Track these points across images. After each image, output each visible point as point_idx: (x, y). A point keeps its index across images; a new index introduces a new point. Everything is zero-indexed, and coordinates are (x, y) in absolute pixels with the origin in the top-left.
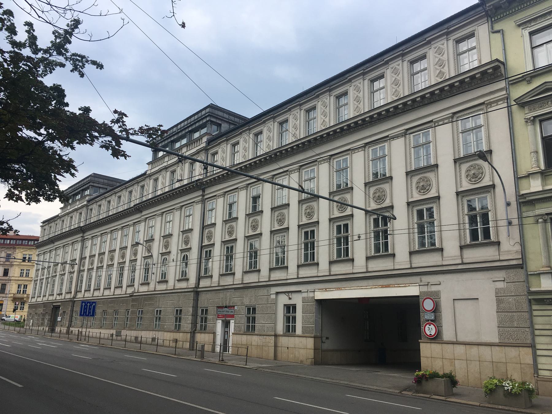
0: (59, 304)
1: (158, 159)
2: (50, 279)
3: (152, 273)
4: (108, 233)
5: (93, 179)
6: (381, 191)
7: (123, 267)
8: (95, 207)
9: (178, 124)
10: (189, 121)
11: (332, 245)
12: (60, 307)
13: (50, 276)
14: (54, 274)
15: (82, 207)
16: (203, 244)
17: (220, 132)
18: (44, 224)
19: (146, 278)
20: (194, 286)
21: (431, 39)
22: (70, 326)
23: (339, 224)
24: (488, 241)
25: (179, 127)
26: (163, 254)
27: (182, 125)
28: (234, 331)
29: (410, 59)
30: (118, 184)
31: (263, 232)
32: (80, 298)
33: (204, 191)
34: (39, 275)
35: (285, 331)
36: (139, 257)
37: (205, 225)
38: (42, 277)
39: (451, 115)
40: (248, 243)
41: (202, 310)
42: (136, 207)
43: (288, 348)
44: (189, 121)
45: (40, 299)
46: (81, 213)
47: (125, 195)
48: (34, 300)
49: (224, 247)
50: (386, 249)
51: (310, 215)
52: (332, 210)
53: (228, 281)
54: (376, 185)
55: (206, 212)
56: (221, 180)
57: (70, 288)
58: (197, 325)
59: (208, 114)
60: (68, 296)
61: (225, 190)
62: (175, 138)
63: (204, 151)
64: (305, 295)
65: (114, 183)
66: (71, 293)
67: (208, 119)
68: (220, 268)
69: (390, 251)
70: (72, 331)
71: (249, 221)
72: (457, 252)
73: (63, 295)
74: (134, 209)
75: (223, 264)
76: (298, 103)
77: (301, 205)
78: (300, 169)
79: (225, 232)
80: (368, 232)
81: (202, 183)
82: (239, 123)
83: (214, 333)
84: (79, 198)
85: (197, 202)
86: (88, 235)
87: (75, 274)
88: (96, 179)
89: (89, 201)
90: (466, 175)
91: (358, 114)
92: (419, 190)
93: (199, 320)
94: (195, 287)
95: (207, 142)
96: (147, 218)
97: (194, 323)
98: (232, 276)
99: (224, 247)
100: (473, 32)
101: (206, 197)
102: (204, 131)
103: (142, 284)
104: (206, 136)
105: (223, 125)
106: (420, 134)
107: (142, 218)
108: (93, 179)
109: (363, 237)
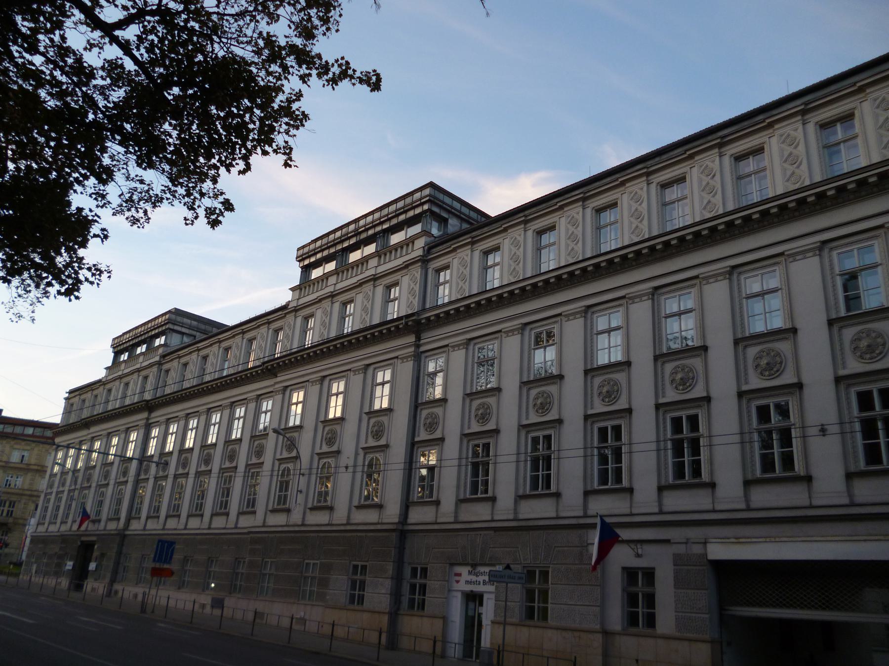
0: (94, 538)
1: (308, 284)
2: (76, 493)
3: (298, 491)
4: (225, 406)
5: (173, 317)
6: (772, 354)
7: (231, 477)
8: (174, 365)
9: (359, 218)
10: (385, 212)
11: (849, 435)
12: (94, 545)
13: (78, 486)
14: (86, 485)
15: (151, 366)
16: (417, 439)
17: (445, 233)
18: (73, 395)
19: (282, 499)
20: (396, 520)
21: (863, 86)
22: (113, 581)
23: (602, 424)
24: (791, 474)
25: (362, 223)
26: (321, 455)
27: (370, 219)
28: (495, 616)
29: (820, 119)
30: (215, 331)
31: (566, 416)
32: (136, 530)
33: (418, 338)
34: (56, 485)
35: (626, 625)
36: (268, 458)
37: (420, 402)
38: (61, 489)
39: (818, 244)
40: (527, 438)
41: (414, 571)
42: (267, 367)
43: (637, 661)
44: (385, 212)
45: (53, 528)
46: (146, 378)
47: (215, 352)
48: (41, 529)
49: (468, 446)
50: (619, 479)
51: (544, 407)
52: (839, 357)
53: (480, 513)
54: (676, 360)
55: (424, 376)
56: (451, 320)
57: (117, 512)
58: (403, 598)
59: (427, 198)
60: (112, 526)
61: (469, 336)
62: (351, 243)
63: (420, 264)
64: (681, 549)
65: (208, 328)
66: (118, 519)
67: (426, 207)
68: (458, 487)
69: (625, 483)
70: (116, 592)
71: (470, 406)
72: (739, 491)
73: (103, 524)
74: (262, 370)
75: (466, 479)
76: (645, 170)
77: (589, 377)
78: (653, 295)
79: (470, 415)
80: (847, 420)
81: (418, 323)
82: (477, 222)
83: (445, 619)
84: (126, 358)
85: (404, 359)
86: (159, 415)
87: (130, 486)
88: (179, 319)
89: (163, 356)
90: (755, 365)
91: (797, 186)
92: (674, 385)
93: (406, 588)
94: (399, 523)
95: (426, 247)
96: (325, 377)
97: (396, 595)
98: (490, 503)
99: (468, 446)
100: (761, 145)
101: (422, 349)
102: (416, 229)
103: (274, 511)
104: (424, 237)
105: (450, 221)
106: (852, 250)
107: (277, 386)
108: (173, 317)
109: (835, 429)
